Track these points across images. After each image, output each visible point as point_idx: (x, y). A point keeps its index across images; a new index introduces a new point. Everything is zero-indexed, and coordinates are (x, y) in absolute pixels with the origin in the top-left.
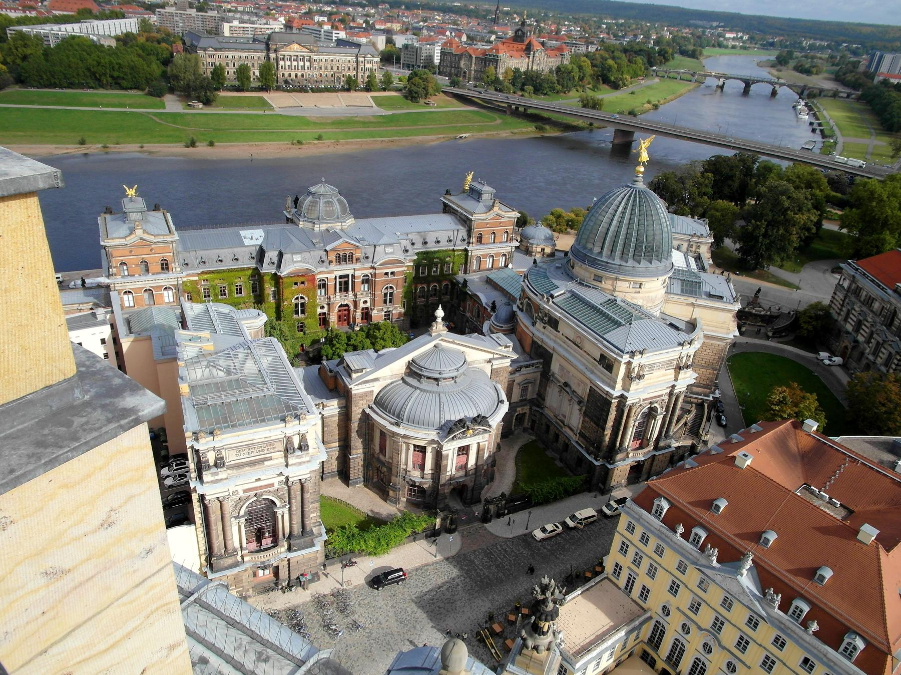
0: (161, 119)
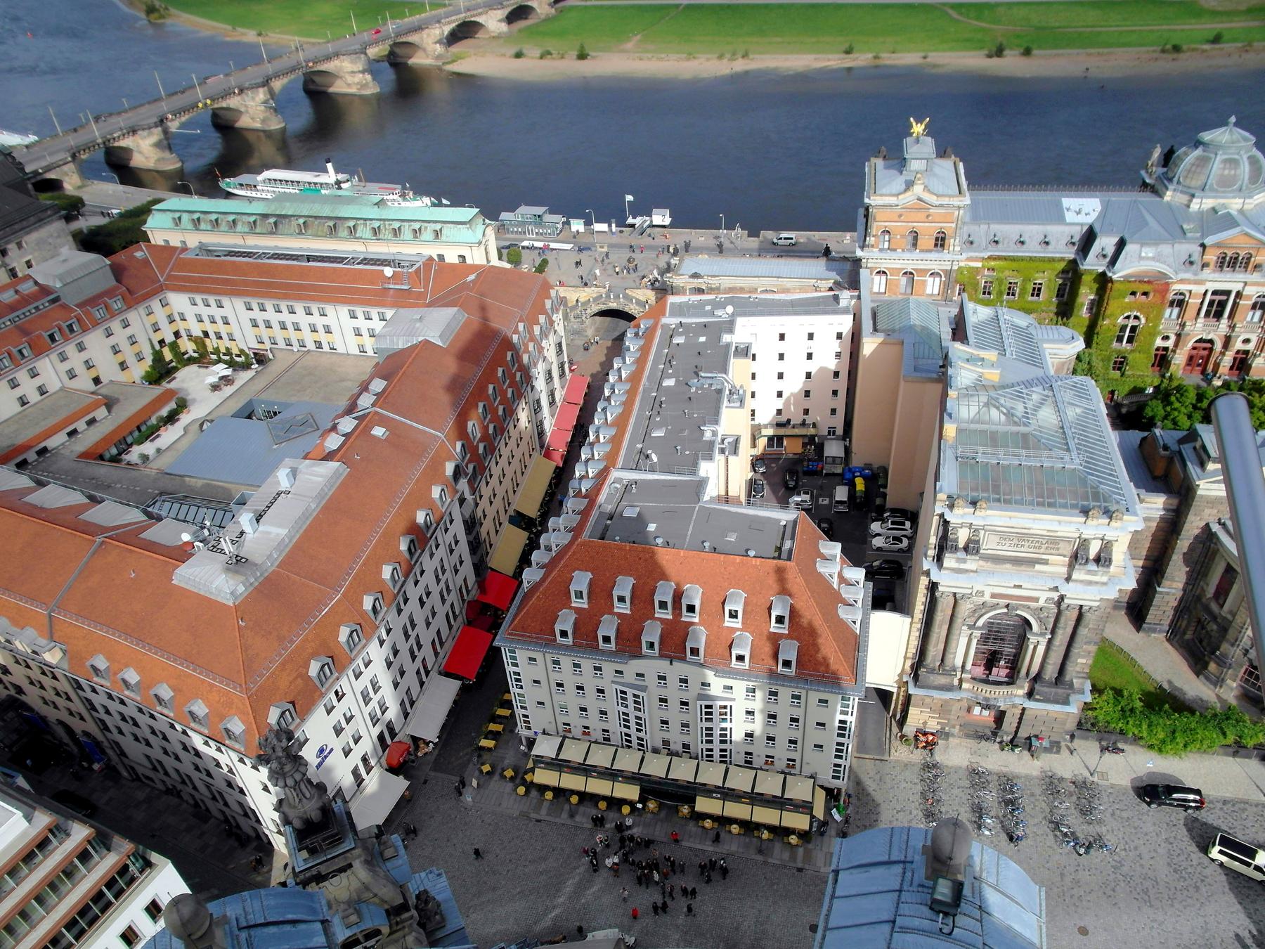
0: (961, 14)
